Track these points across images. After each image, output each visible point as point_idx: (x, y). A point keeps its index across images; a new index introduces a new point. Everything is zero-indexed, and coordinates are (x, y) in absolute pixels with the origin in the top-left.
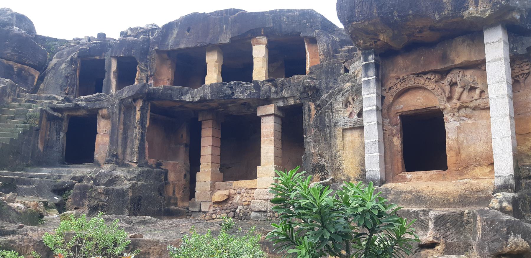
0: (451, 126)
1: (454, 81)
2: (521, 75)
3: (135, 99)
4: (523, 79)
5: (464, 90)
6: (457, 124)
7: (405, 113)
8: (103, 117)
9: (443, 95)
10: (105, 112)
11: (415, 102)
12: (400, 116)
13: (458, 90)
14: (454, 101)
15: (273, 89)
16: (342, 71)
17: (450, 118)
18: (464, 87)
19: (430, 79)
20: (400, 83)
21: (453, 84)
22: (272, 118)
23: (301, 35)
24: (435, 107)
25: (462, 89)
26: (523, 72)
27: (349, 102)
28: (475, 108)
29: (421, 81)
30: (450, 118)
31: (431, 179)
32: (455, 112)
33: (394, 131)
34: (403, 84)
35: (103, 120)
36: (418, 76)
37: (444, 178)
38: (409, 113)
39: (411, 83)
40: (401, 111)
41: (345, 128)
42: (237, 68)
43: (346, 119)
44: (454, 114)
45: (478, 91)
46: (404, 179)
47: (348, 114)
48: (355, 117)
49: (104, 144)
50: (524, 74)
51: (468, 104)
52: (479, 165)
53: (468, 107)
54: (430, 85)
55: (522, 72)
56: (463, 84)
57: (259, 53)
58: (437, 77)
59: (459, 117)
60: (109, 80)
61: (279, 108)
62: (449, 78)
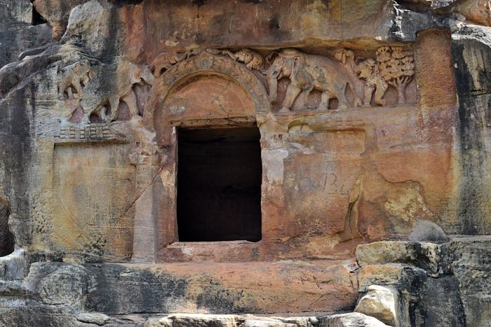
1: (286, 72)
2: (401, 78)
4: (404, 85)
5: (302, 91)
7: (188, 124)
9: (265, 97)
11: (208, 104)
12: (179, 129)
13: (292, 91)
14: (284, 110)
16: (27, 17)
17: (273, 143)
19: (243, 62)
20: (184, 62)
24: (246, 118)
25: (298, 91)
26: (405, 73)
27: (72, 86)
29: (226, 64)
30: (273, 143)
31: (230, 258)
32: (284, 131)
33: (165, 158)
34: (190, 66)
36: (220, 54)
38: (195, 124)
40: (180, 118)
41: (59, 141)
43: (65, 122)
44: (280, 136)
45: (325, 98)
46: (178, 257)
47: (68, 112)
48: (84, 122)
50: (405, 77)
51: (307, 120)
52: (319, 233)
53: (307, 124)
54: (244, 76)
55: (402, 73)
56: (302, 80)
58: (255, 61)
59: (288, 141)
62: (277, 64)
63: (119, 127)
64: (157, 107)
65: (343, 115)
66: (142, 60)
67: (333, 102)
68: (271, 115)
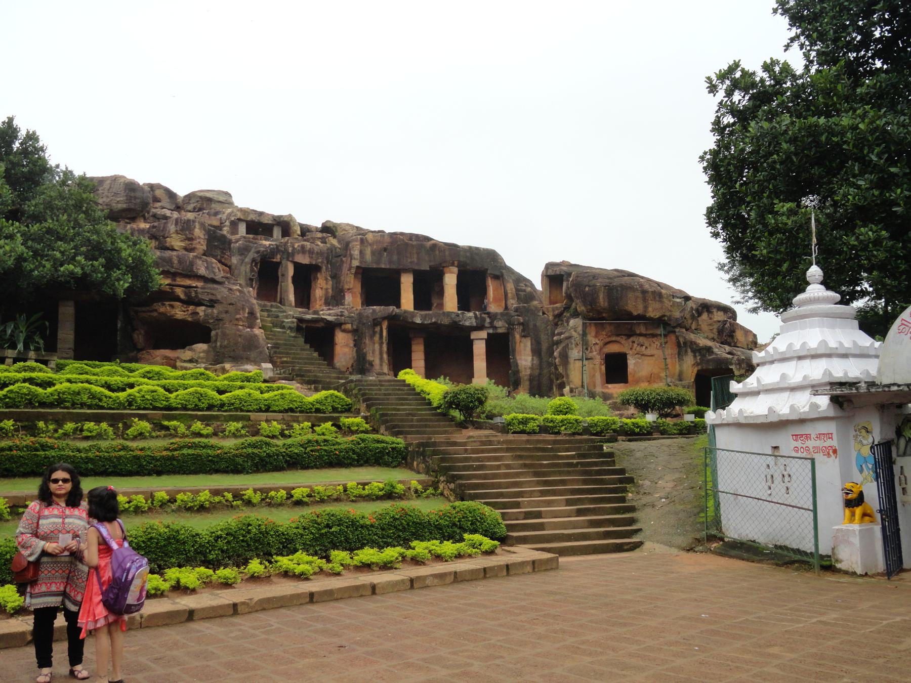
0: (631, 362)
3: (384, 318)
8: (344, 331)
10: (349, 326)
11: (614, 348)
13: (635, 345)
15: (488, 320)
16: (541, 314)
21: (633, 342)
22: (484, 341)
28: (643, 355)
29: (618, 339)
39: (614, 339)
46: (607, 388)
49: (345, 354)
54: (623, 342)
57: (450, 280)
60: (287, 286)
61: (488, 334)
62: (632, 339)
64: (601, 349)
65: (648, 352)
66: (596, 336)
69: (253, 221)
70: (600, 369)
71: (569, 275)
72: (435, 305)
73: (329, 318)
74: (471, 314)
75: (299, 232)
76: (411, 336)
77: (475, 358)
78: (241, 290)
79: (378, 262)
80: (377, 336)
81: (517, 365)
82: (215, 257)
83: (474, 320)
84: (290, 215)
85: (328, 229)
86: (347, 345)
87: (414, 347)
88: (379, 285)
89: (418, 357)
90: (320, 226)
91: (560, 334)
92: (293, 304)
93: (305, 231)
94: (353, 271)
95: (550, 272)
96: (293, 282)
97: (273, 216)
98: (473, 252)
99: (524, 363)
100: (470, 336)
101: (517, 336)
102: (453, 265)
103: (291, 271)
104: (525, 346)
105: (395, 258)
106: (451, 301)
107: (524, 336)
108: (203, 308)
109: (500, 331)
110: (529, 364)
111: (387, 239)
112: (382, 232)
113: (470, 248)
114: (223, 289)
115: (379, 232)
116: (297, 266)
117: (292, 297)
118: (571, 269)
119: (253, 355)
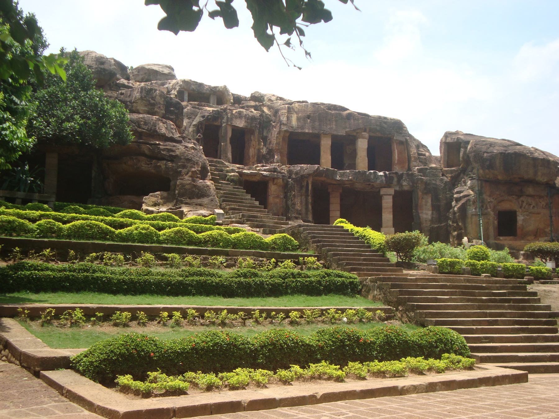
0: (520, 218)
6: (523, 218)
11: (506, 206)
13: (524, 204)
18: (527, 204)
21: (523, 202)
22: (391, 197)
23: (395, 138)
31: (510, 240)
35: (273, 186)
37: (516, 240)
42: (343, 151)
46: (500, 240)
57: (362, 145)
61: (395, 191)
62: (521, 199)
63: (486, 211)
64: (494, 207)
66: (490, 196)
67: (534, 207)
68: (520, 210)
69: (193, 90)
70: (494, 223)
71: (468, 143)
72: (347, 165)
73: (265, 173)
74: (381, 173)
75: (232, 101)
76: (329, 190)
77: (383, 210)
78: (191, 148)
79: (302, 127)
80: (304, 189)
81: (419, 218)
82: (171, 120)
83: (384, 178)
84: (225, 87)
85: (257, 98)
86: (278, 197)
87: (332, 200)
88: (301, 147)
89: (335, 206)
90: (248, 95)
91: (458, 192)
92: (231, 161)
93: (238, 100)
94: (282, 134)
95: (449, 140)
96: (231, 143)
97: (210, 86)
98: (382, 121)
99: (425, 216)
100: (379, 191)
101: (420, 193)
102: (365, 131)
103: (229, 134)
104: (427, 202)
105: (317, 124)
106: (362, 162)
107: (426, 194)
108: (165, 162)
109: (406, 188)
110: (429, 217)
111: (310, 109)
112: (306, 102)
113: (380, 117)
114: (181, 147)
115: (303, 102)
116: (235, 130)
117: (230, 155)
118: (468, 138)
119: (205, 200)
